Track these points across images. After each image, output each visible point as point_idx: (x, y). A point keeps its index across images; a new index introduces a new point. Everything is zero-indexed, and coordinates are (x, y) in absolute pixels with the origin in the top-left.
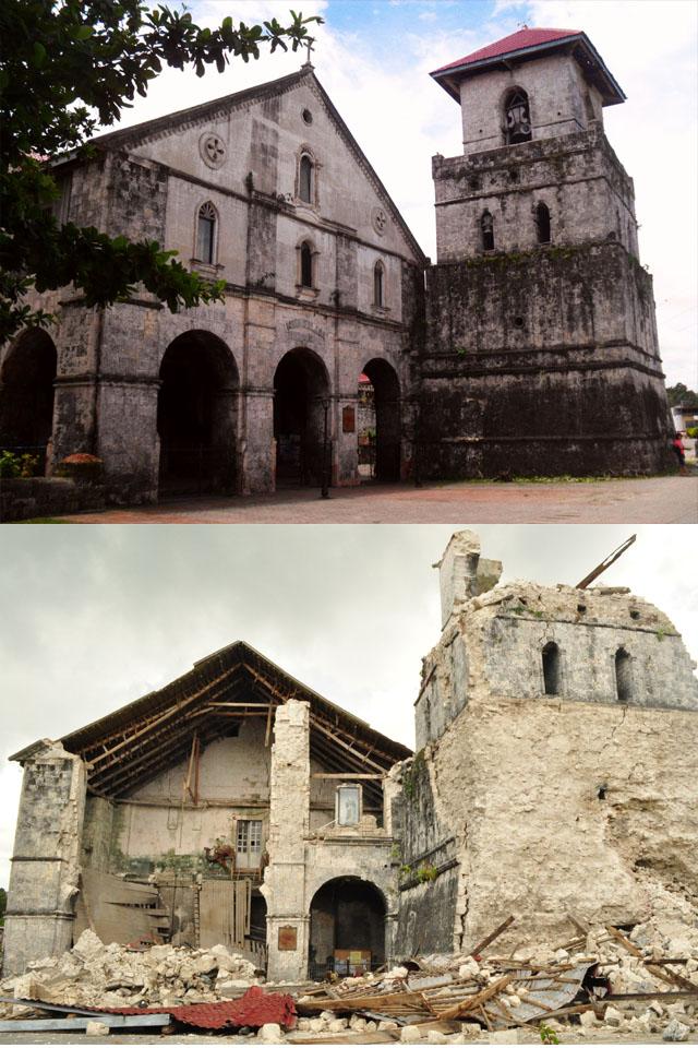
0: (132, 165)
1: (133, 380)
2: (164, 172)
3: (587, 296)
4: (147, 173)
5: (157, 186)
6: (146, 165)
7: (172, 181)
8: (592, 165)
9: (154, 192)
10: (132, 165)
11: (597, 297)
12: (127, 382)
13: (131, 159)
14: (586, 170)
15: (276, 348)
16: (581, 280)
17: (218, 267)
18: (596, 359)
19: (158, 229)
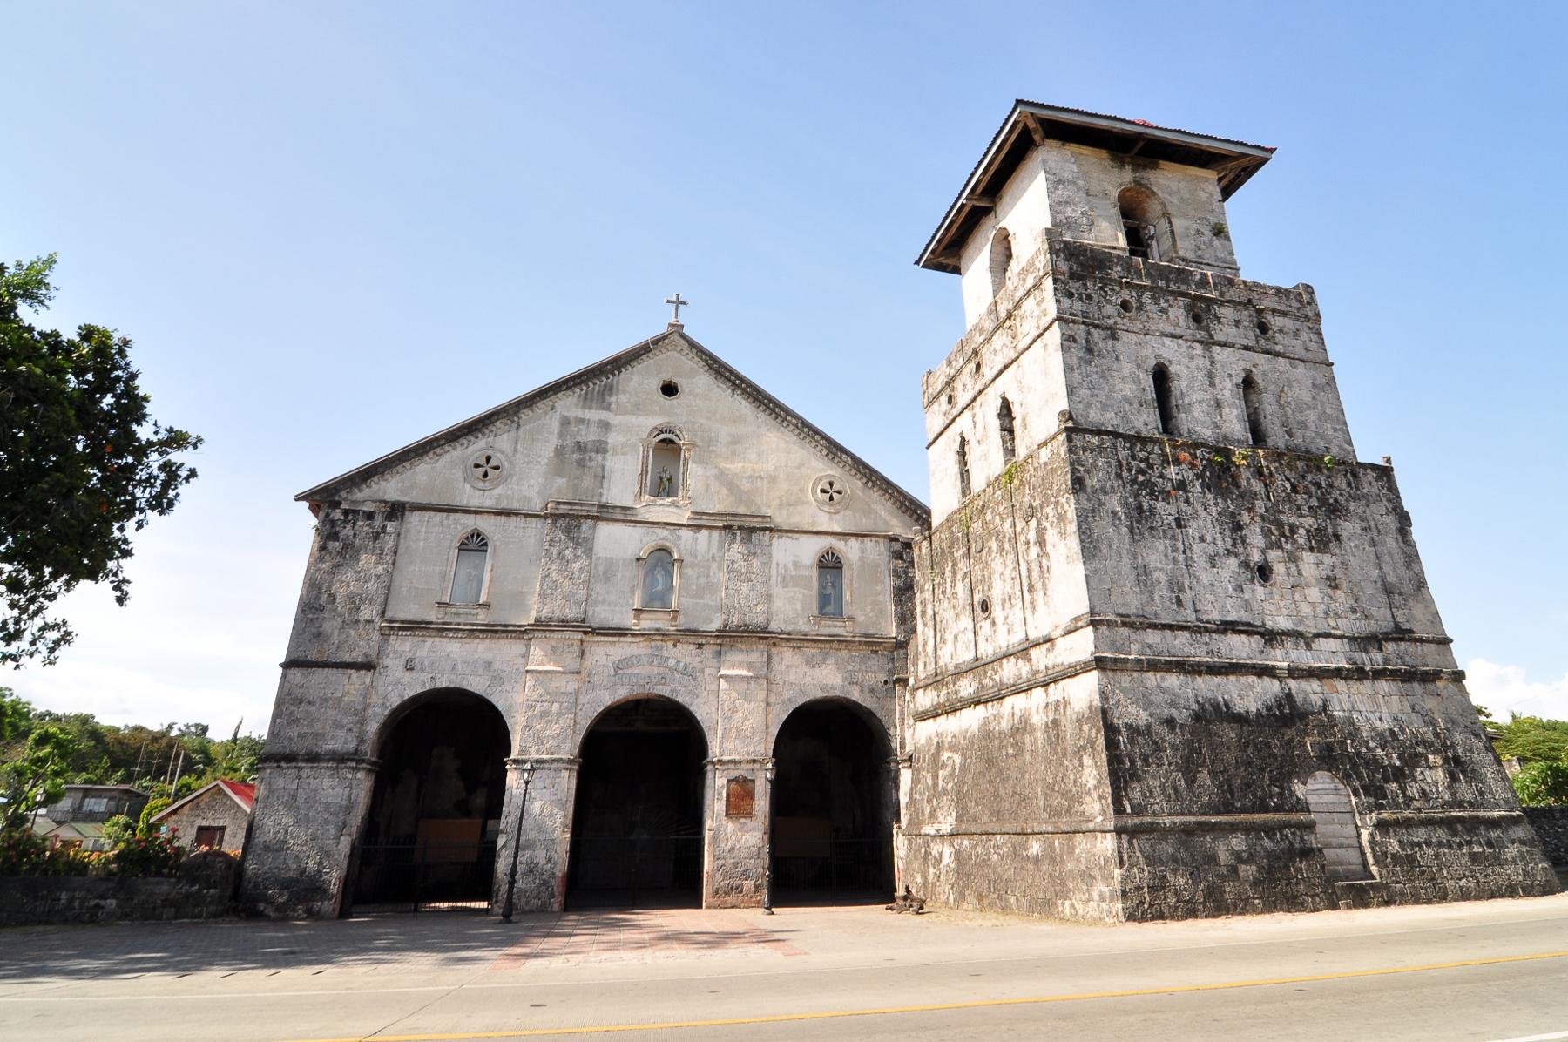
0: (346, 513)
1: (313, 758)
2: (396, 510)
3: (1041, 542)
4: (370, 516)
5: (384, 527)
6: (368, 507)
7: (414, 518)
8: (1044, 305)
9: (376, 537)
10: (346, 513)
11: (1051, 535)
12: (307, 761)
13: (344, 506)
14: (1039, 318)
15: (582, 699)
16: (1031, 513)
17: (487, 605)
18: (1059, 661)
19: (378, 577)
